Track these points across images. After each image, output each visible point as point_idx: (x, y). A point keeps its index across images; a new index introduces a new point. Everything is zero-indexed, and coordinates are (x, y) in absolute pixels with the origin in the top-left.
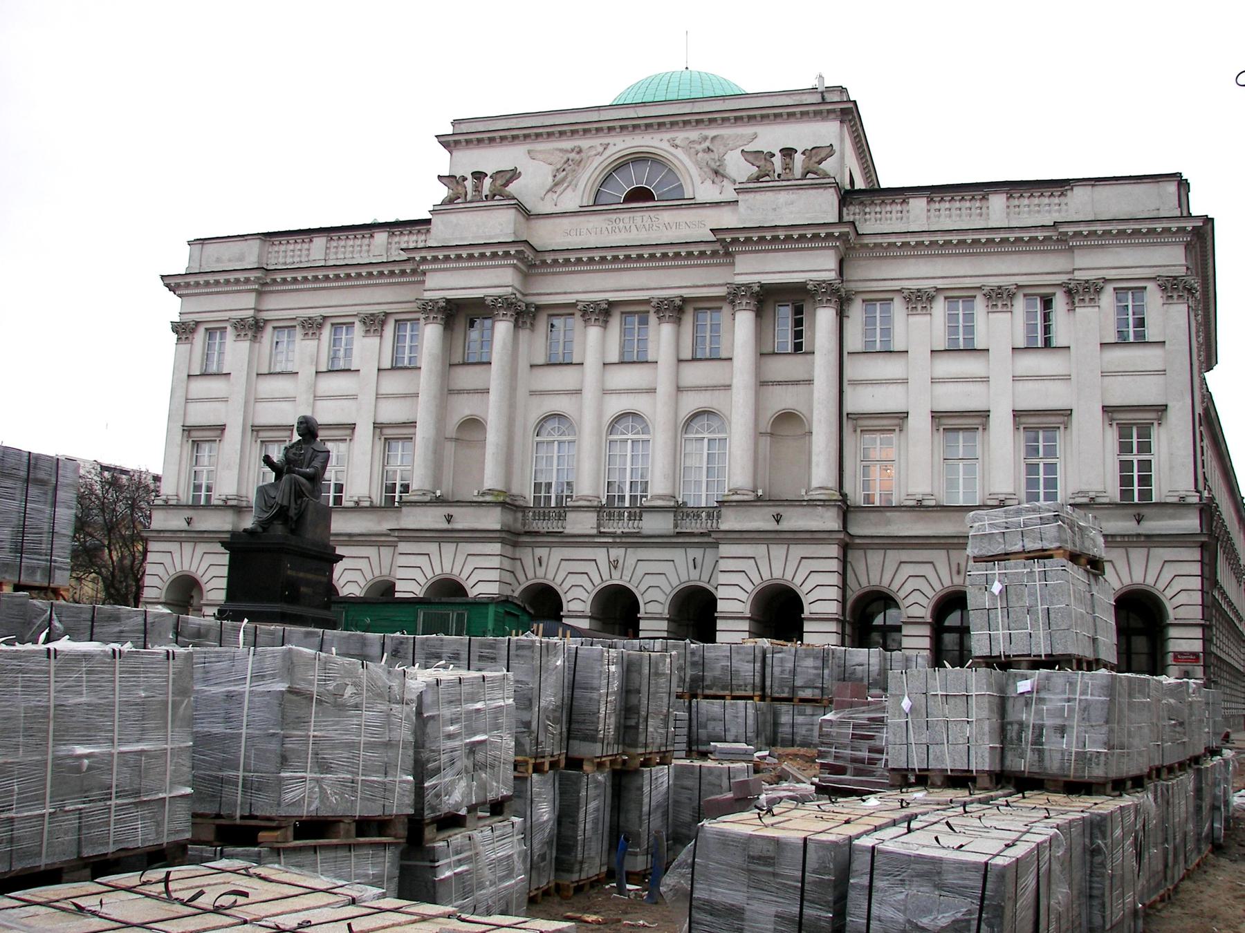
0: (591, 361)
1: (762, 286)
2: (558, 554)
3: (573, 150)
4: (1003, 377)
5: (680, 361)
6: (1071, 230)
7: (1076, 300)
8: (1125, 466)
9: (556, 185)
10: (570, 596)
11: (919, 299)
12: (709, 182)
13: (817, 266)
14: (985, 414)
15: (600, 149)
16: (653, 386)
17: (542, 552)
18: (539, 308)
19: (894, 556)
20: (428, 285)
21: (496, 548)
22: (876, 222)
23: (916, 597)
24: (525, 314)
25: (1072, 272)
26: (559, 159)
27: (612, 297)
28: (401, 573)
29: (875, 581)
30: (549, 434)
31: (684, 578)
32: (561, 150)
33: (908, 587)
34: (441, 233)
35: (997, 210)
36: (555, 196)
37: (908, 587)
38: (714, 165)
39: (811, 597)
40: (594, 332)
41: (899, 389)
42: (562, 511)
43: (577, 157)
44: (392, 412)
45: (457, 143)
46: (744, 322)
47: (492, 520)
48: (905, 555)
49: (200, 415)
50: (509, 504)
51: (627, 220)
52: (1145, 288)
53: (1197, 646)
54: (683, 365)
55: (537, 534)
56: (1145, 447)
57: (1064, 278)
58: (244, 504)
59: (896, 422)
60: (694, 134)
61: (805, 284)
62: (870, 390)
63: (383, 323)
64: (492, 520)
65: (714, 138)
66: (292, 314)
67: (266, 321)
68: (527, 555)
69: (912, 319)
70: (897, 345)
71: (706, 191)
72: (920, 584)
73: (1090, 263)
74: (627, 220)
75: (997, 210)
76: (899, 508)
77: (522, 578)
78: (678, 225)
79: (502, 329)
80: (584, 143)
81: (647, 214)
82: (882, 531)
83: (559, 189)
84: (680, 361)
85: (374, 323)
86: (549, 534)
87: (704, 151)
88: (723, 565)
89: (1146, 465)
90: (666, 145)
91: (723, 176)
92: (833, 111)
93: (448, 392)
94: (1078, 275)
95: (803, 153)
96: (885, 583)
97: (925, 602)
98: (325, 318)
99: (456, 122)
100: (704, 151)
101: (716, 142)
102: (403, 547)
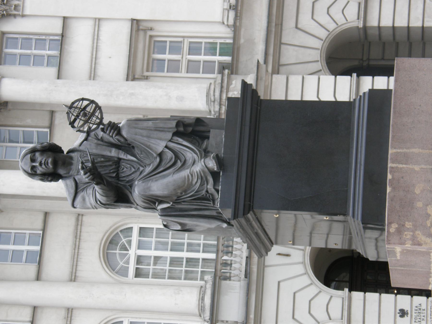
5: (38, 278)
16: (63, 313)
19: (289, 35)
29: (316, 55)
31: (300, 269)
33: (324, 19)
37: (324, 19)
41: (106, 29)
48: (289, 23)
54: (44, 275)
59: (141, 34)
62: (103, 61)
69: (27, 12)
70: (56, 27)
76: (236, 29)
82: (260, 47)
84: (38, 278)
96: (318, 44)
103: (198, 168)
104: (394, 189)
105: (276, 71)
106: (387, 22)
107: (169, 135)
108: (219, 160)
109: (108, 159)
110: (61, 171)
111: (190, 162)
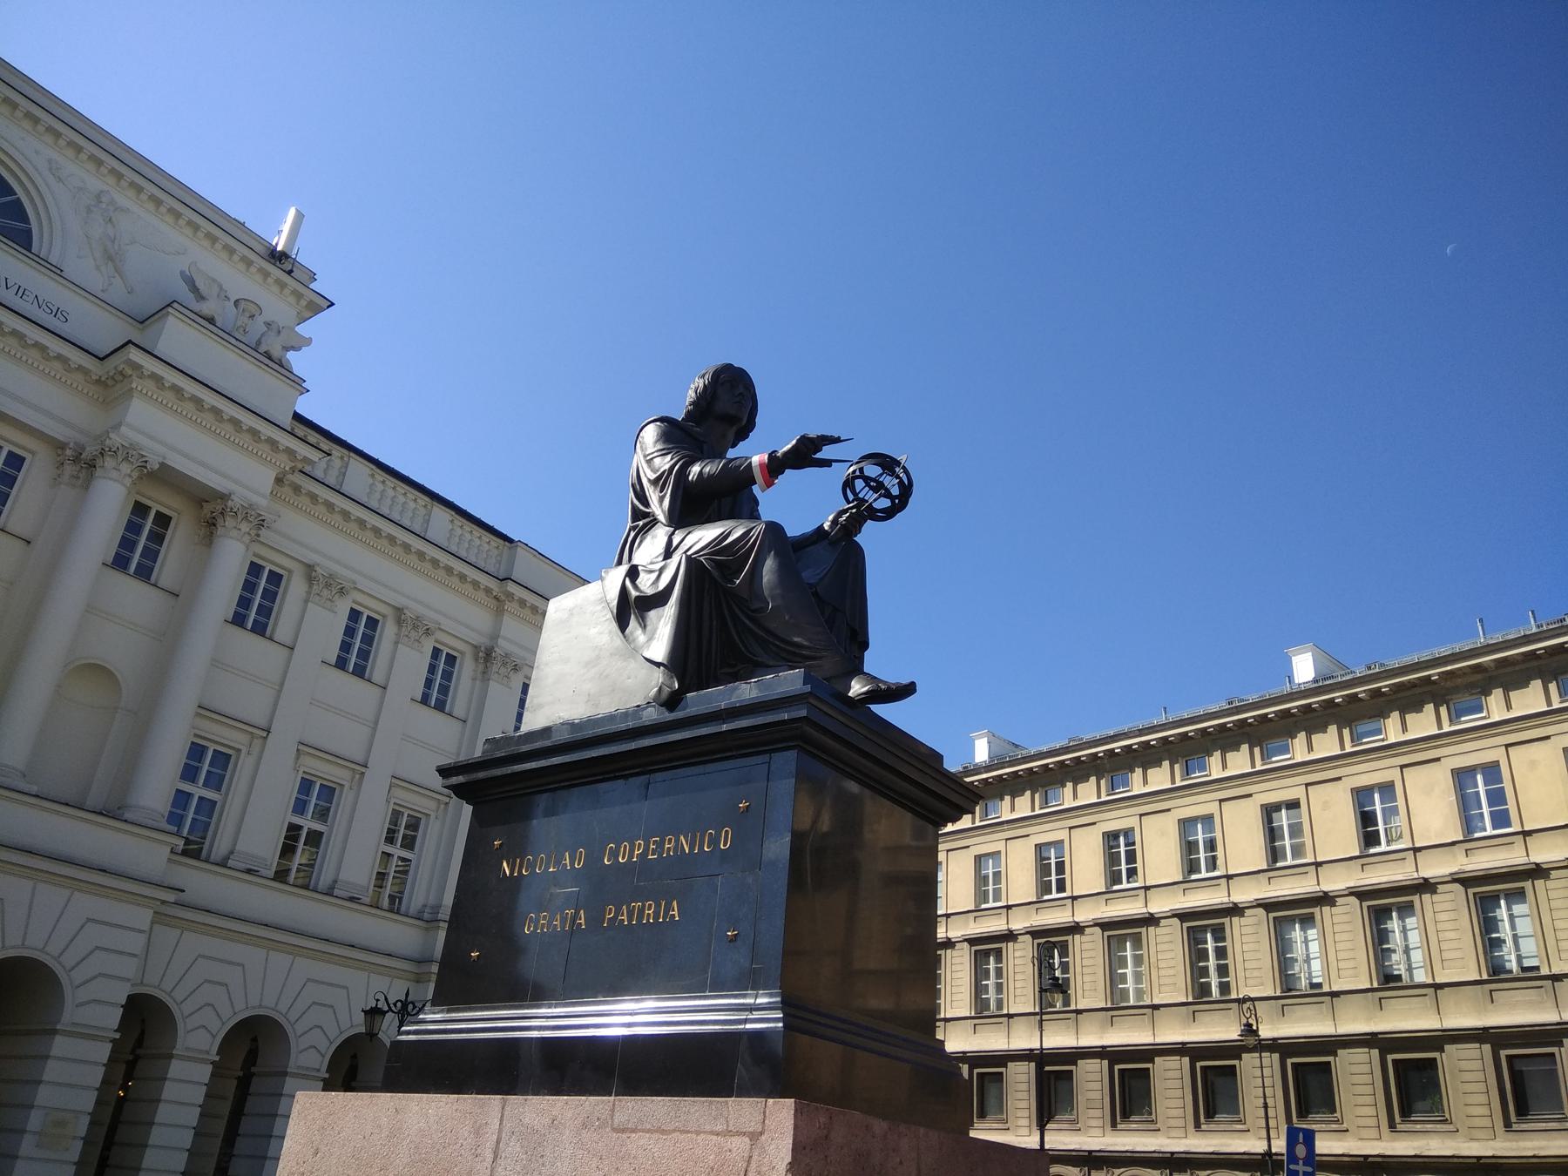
1: (163, 465)
61: (224, 497)
95: (268, 324)
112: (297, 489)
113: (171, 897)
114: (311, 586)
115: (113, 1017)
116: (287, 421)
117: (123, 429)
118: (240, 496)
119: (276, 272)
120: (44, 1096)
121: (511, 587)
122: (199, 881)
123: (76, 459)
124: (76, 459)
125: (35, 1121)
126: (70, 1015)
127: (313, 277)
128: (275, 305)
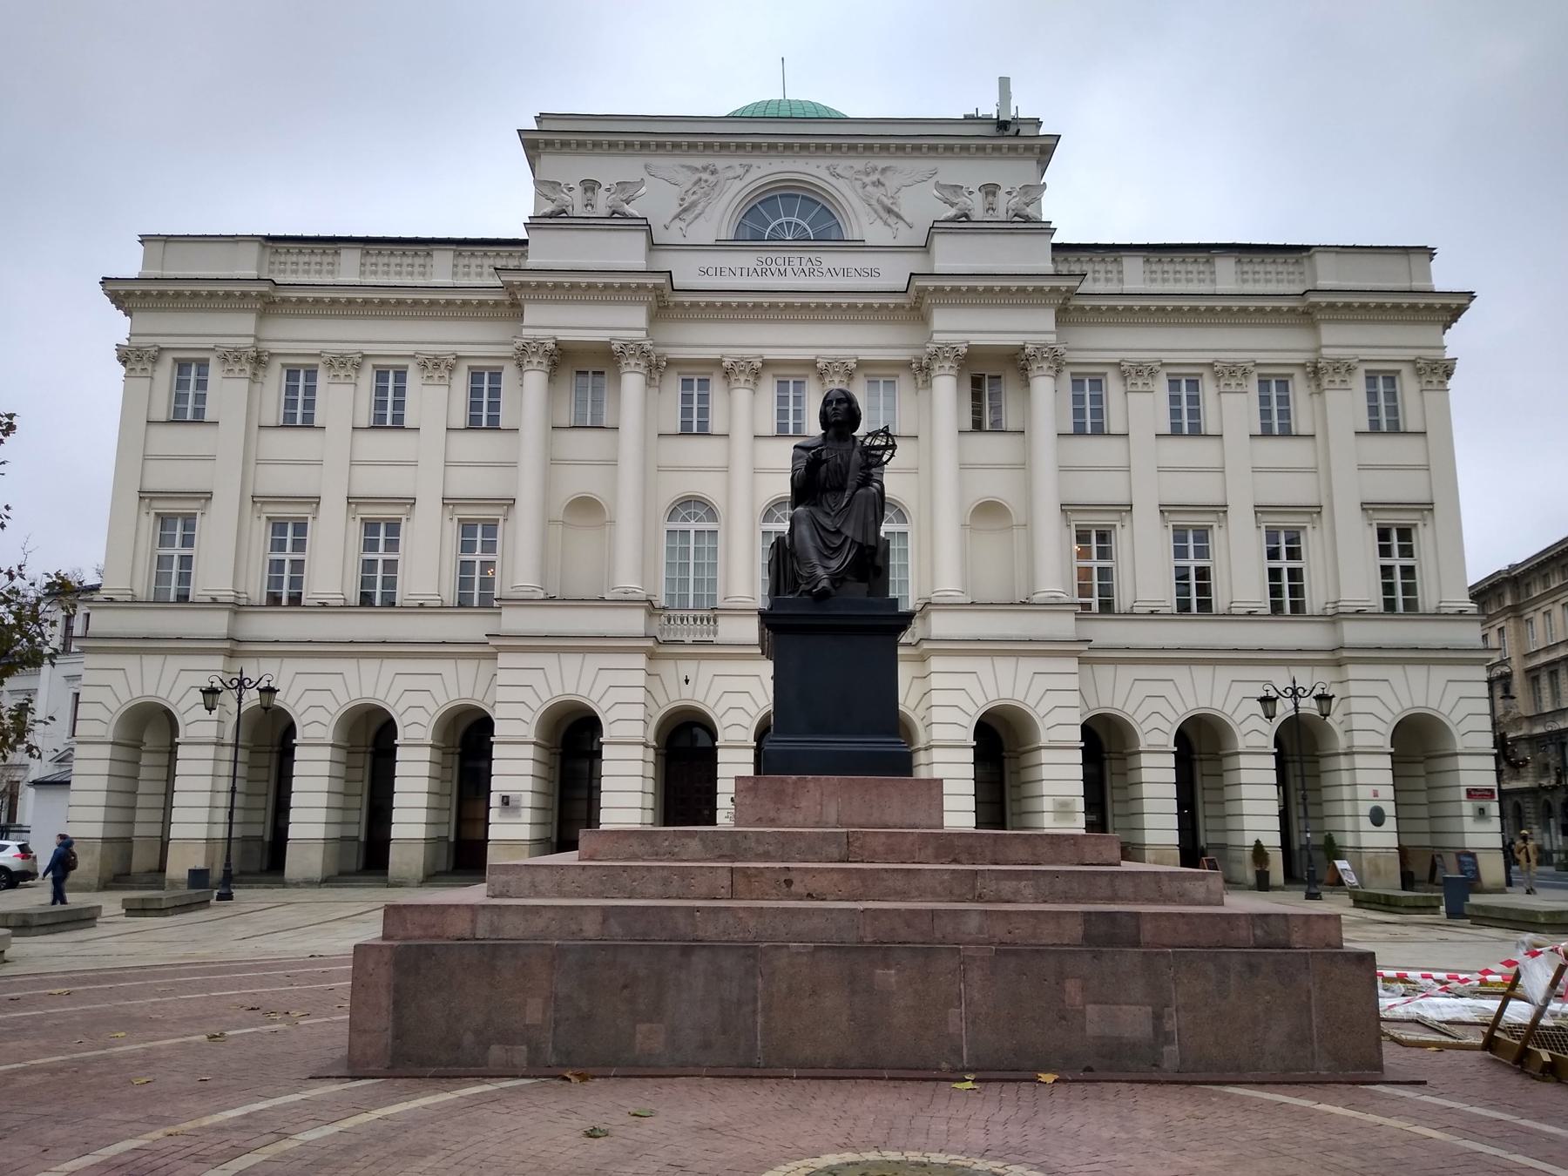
0: (742, 436)
2: (709, 668)
3: (705, 169)
4: (1239, 469)
6: (1323, 300)
7: (1325, 384)
8: (1387, 571)
9: (685, 210)
10: (726, 721)
11: (1136, 373)
12: (879, 223)
13: (1030, 327)
14: (1221, 510)
15: (740, 171)
17: (687, 668)
18: (671, 363)
19: (1127, 673)
20: (527, 320)
21: (640, 661)
22: (1098, 281)
23: (1157, 721)
24: (656, 368)
25: (1317, 349)
26: (687, 179)
27: (771, 354)
28: (501, 694)
30: (684, 519)
32: (689, 168)
34: (549, 252)
35: (1226, 277)
36: (683, 225)
38: (888, 202)
39: (1050, 721)
40: (742, 396)
42: (714, 614)
43: (712, 179)
44: (469, 483)
45: (549, 143)
46: (946, 387)
47: (634, 622)
49: (164, 477)
50: (651, 607)
51: (780, 261)
52: (1398, 372)
53: (1489, 780)
55: (681, 643)
56: (1407, 551)
57: (1310, 356)
58: (243, 602)
60: (859, 164)
61: (1023, 348)
63: (451, 369)
64: (634, 622)
65: (884, 170)
66: (315, 348)
67: (271, 355)
68: (667, 669)
71: (875, 233)
72: (1160, 705)
73: (1337, 340)
74: (780, 261)
75: (1226, 277)
77: (662, 700)
78: (846, 273)
79: (633, 382)
80: (720, 163)
81: (806, 256)
83: (689, 217)
85: (439, 367)
86: (696, 643)
87: (873, 184)
88: (935, 681)
89: (1408, 571)
90: (825, 174)
91: (898, 216)
92: (1029, 148)
93: (552, 461)
94: (1325, 351)
95: (1009, 193)
97: (1166, 727)
98: (364, 356)
99: (541, 118)
100: (873, 184)
101: (889, 173)
102: (503, 659)
103: (820, 572)
104: (795, 783)
105: (1083, 661)
106: (1146, 775)
107: (859, 539)
108: (824, 594)
109: (845, 480)
110: (831, 432)
111: (827, 563)
112: (1082, 308)
113: (1084, 647)
114: (1125, 379)
115: (1077, 734)
116: (1047, 266)
117: (936, 337)
118: (1031, 341)
119: (1005, 142)
120: (1046, 788)
121: (1314, 299)
122: (1106, 632)
123: (921, 369)
124: (921, 369)
125: (1047, 804)
126: (1044, 738)
127: (1037, 123)
128: (1008, 173)
